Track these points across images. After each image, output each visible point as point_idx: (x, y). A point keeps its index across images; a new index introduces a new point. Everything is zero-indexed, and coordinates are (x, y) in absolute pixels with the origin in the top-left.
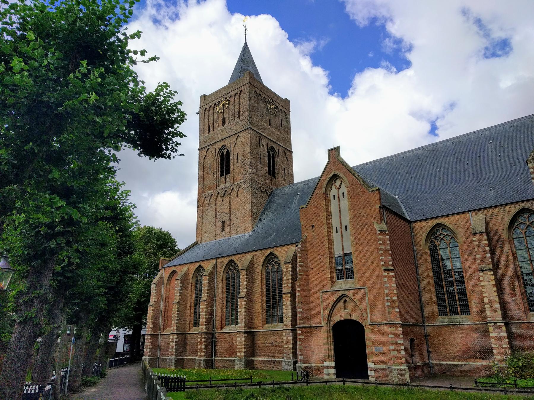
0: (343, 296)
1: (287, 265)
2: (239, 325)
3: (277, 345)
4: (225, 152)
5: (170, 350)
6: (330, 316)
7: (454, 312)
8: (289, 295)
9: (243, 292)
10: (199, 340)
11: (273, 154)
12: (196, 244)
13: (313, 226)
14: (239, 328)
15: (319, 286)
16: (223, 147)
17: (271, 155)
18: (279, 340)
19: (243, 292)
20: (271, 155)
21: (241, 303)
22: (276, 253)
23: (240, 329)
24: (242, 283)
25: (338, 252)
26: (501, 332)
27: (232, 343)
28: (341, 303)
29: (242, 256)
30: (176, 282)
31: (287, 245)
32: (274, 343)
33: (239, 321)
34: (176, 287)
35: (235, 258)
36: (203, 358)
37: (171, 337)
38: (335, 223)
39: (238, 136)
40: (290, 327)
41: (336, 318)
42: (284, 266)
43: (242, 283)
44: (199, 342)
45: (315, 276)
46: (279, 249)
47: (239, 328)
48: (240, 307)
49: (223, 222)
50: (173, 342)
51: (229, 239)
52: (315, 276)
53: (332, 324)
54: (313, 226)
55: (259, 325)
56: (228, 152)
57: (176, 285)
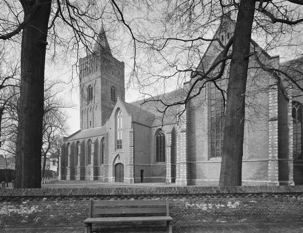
0: (118, 155)
4: (91, 88)
6: (114, 162)
7: (161, 161)
9: (93, 151)
12: (80, 131)
19: (93, 151)
25: (118, 139)
26: (170, 168)
28: (118, 158)
35: (91, 138)
36: (79, 176)
38: (118, 128)
41: (116, 163)
49: (91, 121)
53: (115, 164)
54: (110, 128)
55: (100, 165)
56: (92, 88)
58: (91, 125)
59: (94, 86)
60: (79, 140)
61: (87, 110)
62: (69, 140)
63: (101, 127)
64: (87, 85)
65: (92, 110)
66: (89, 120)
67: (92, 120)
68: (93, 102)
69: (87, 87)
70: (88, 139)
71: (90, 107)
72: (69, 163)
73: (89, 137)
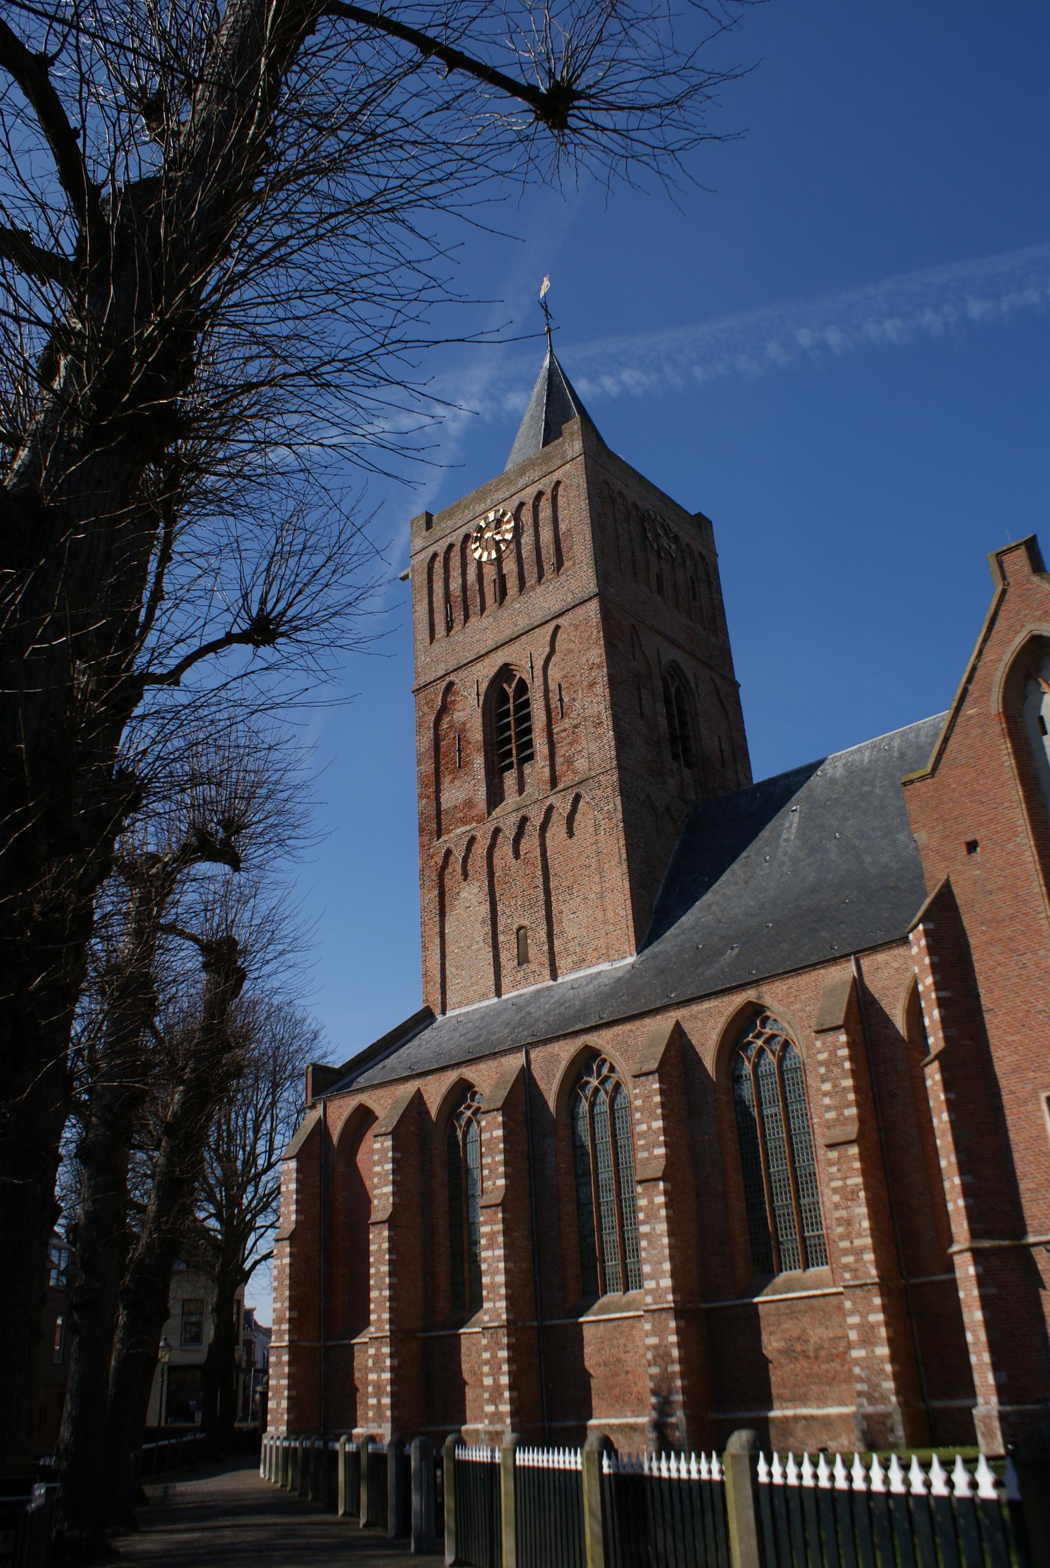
1: (830, 1037)
2: (650, 1284)
3: (811, 1354)
5: (373, 1401)
8: (854, 1150)
10: (486, 1355)
11: (678, 689)
13: (972, 846)
14: (649, 1299)
15: (1031, 1075)
16: (506, 672)
17: (673, 690)
18: (818, 1334)
20: (673, 690)
21: (651, 1202)
22: (768, 1001)
23: (655, 1303)
24: (644, 1127)
27: (619, 1360)
29: (628, 1027)
30: (377, 1146)
31: (814, 966)
32: (798, 1348)
33: (646, 1269)
34: (379, 1163)
37: (372, 1351)
39: (558, 627)
40: (869, 1275)
42: (818, 1044)
43: (644, 1127)
44: (487, 1362)
45: (1009, 1038)
46: (780, 987)
47: (649, 1299)
48: (647, 1216)
50: (383, 1371)
51: (549, 988)
52: (1009, 1038)
57: (376, 1157)
58: (523, 959)
59: (538, 673)
60: (469, 1073)
61: (480, 848)
62: (362, 1081)
63: (630, 960)
64: (486, 670)
65: (530, 844)
66: (502, 920)
67: (533, 920)
68: (538, 770)
69: (484, 686)
70: (565, 1051)
71: (514, 819)
72: (379, 1294)
73: (576, 1034)
